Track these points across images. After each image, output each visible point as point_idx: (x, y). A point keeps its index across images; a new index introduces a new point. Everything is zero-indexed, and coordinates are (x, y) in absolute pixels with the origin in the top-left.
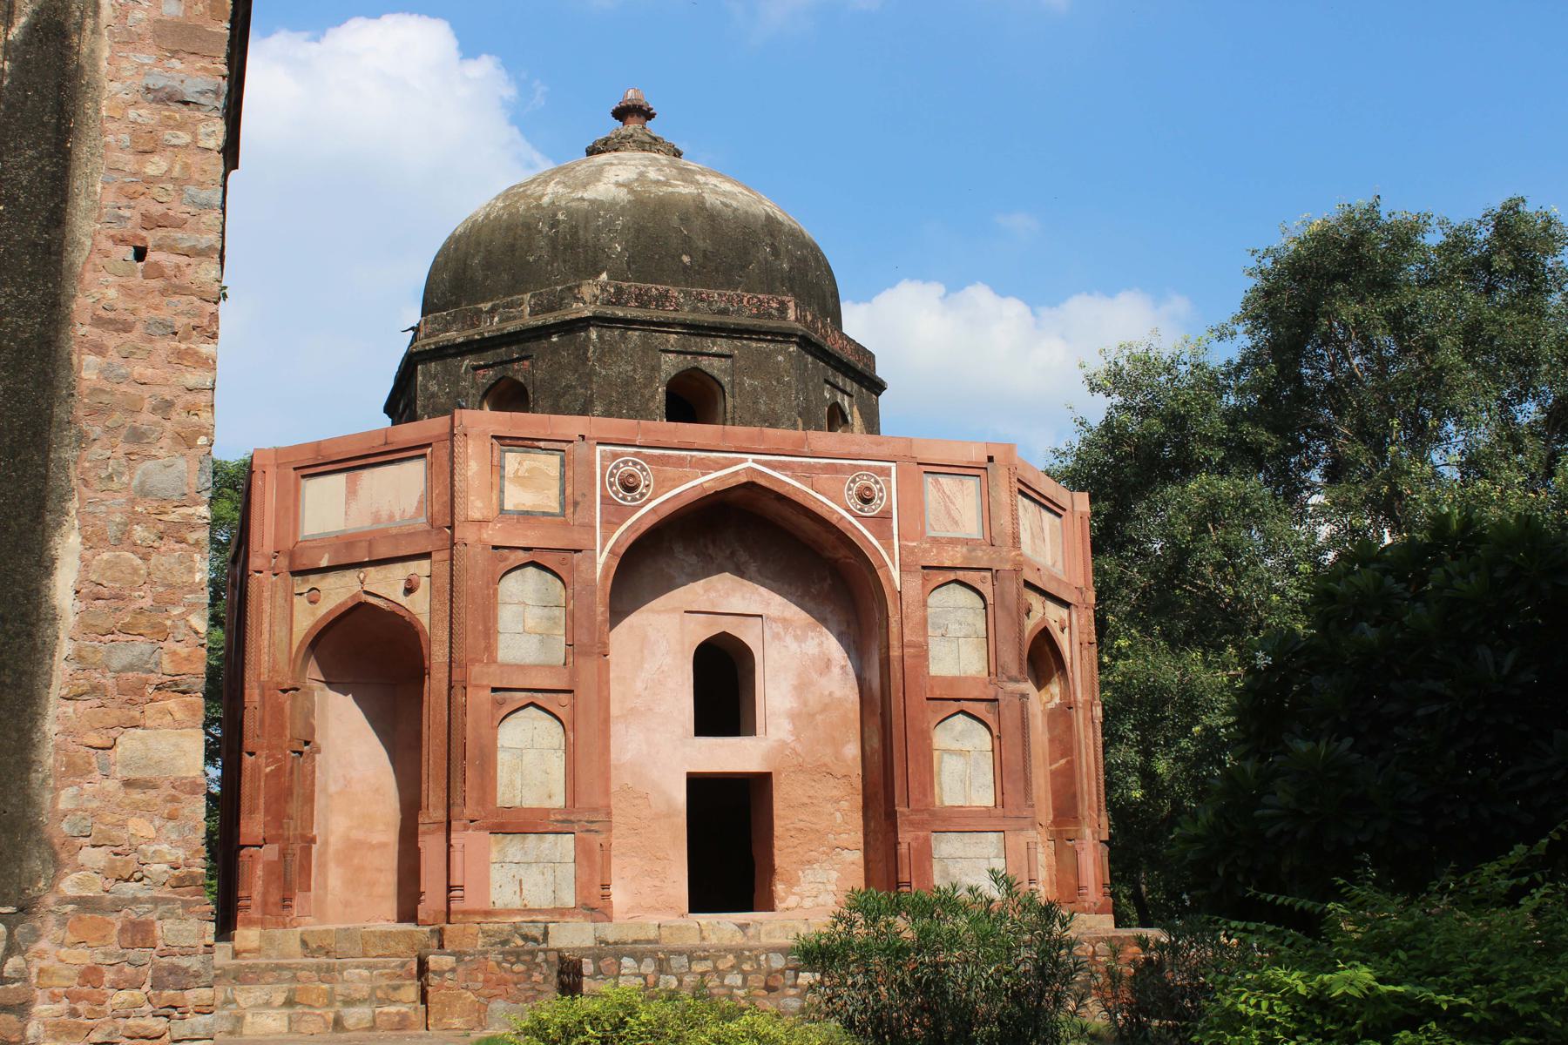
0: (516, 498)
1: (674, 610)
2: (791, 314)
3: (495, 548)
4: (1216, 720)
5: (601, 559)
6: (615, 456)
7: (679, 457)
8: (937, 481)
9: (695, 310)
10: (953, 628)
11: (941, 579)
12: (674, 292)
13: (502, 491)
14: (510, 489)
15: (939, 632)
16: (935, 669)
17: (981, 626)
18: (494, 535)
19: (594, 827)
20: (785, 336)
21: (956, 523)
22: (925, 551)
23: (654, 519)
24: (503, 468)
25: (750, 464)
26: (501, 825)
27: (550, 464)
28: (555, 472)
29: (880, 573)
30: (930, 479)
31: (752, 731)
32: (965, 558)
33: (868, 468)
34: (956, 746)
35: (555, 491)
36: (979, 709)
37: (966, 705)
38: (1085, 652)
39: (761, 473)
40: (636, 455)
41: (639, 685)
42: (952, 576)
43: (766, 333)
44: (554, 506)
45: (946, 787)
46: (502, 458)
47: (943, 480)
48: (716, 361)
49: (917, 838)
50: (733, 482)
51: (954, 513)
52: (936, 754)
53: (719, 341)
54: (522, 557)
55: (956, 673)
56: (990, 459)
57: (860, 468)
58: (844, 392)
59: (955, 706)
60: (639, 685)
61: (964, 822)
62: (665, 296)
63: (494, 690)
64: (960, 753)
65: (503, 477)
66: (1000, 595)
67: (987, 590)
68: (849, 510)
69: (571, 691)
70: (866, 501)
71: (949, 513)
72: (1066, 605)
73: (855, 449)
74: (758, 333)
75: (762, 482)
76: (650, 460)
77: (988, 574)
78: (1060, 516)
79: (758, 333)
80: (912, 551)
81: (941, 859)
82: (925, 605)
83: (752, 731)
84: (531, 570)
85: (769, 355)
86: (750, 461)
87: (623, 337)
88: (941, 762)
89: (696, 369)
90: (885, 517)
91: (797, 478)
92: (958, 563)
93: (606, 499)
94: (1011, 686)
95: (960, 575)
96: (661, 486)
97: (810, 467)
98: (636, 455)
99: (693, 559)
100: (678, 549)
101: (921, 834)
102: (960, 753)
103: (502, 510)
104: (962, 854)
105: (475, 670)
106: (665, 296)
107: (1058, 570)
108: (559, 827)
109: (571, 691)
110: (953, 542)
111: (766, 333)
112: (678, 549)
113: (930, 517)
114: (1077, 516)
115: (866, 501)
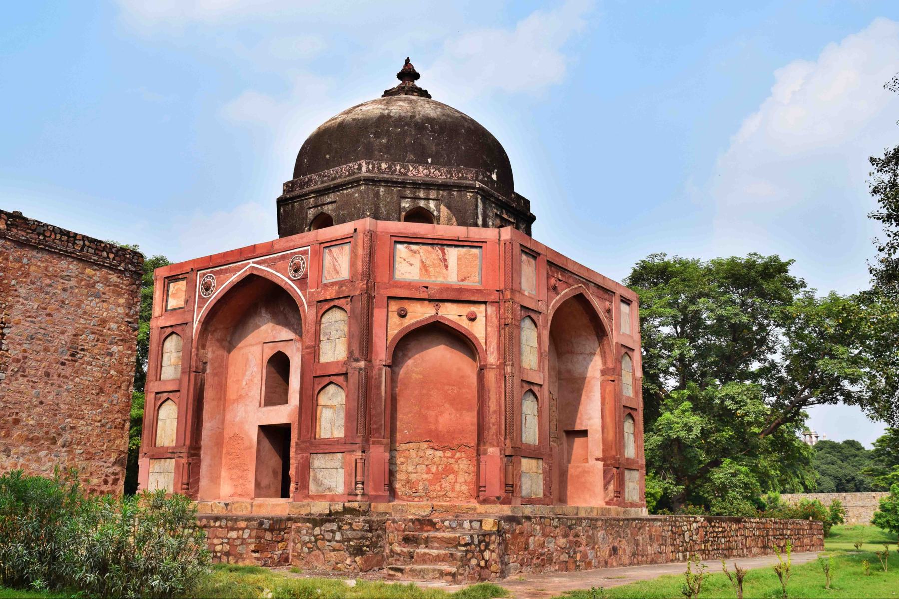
0: (172, 303)
1: (259, 343)
2: (364, 169)
3: (162, 328)
4: (777, 358)
5: (196, 325)
6: (204, 274)
7: (226, 269)
8: (330, 251)
9: (322, 182)
10: (333, 333)
11: (327, 307)
12: (314, 176)
13: (167, 301)
14: (170, 299)
15: (326, 338)
16: (323, 359)
17: (346, 330)
18: (162, 323)
19: (182, 455)
20: (356, 183)
21: (338, 272)
22: (319, 292)
23: (215, 302)
24: (168, 291)
25: (252, 264)
26: (153, 455)
27: (182, 284)
28: (184, 288)
29: (300, 309)
30: (326, 250)
31: (286, 403)
32: (337, 292)
33: (299, 252)
34: (329, 403)
35: (183, 298)
36: (340, 380)
37: (333, 379)
38: (503, 332)
39: (256, 268)
40: (211, 272)
41: (244, 383)
42: (332, 304)
43: (348, 184)
44: (182, 304)
45: (322, 427)
46: (168, 287)
47: (333, 249)
48: (330, 206)
49: (302, 458)
50: (244, 276)
51: (338, 267)
52: (319, 408)
53: (331, 195)
54: (169, 331)
55: (332, 360)
56: (355, 230)
57: (295, 253)
58: (427, 199)
59: (326, 380)
60: (244, 383)
61: (329, 447)
62: (310, 180)
63: (157, 393)
64: (331, 407)
65: (168, 295)
66: (352, 310)
67: (348, 308)
68: (289, 278)
69: (178, 391)
70: (296, 270)
71: (334, 265)
72: (485, 303)
73: (292, 244)
74: (344, 185)
75: (255, 272)
76: (215, 273)
77: (348, 299)
78: (481, 247)
79: (344, 185)
80: (312, 294)
81: (314, 470)
82: (318, 322)
83: (286, 403)
84: (174, 336)
85: (352, 195)
86: (251, 263)
87: (293, 206)
88: (321, 413)
89: (322, 213)
90: (305, 277)
91: (268, 266)
92: (333, 296)
93: (200, 295)
94: (355, 364)
95: (336, 303)
96: (220, 283)
97: (275, 258)
98: (211, 272)
99: (268, 317)
100: (263, 311)
101: (305, 455)
102: (331, 407)
103: (166, 310)
104: (324, 466)
105: (151, 385)
106: (310, 180)
107: (474, 281)
108: (170, 455)
109: (178, 391)
110: (333, 284)
111: (348, 184)
112: (263, 311)
113: (325, 272)
114: (502, 243)
115: (296, 270)
